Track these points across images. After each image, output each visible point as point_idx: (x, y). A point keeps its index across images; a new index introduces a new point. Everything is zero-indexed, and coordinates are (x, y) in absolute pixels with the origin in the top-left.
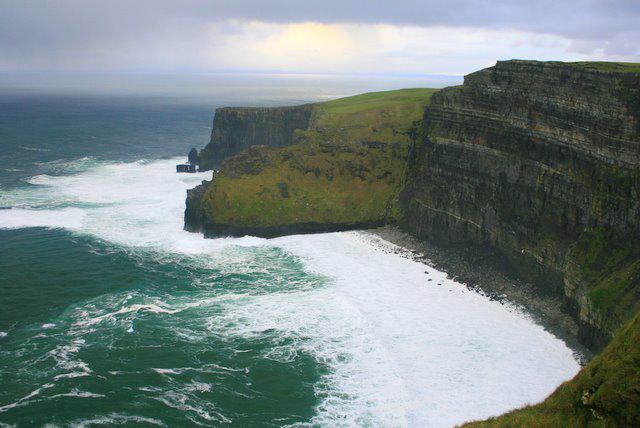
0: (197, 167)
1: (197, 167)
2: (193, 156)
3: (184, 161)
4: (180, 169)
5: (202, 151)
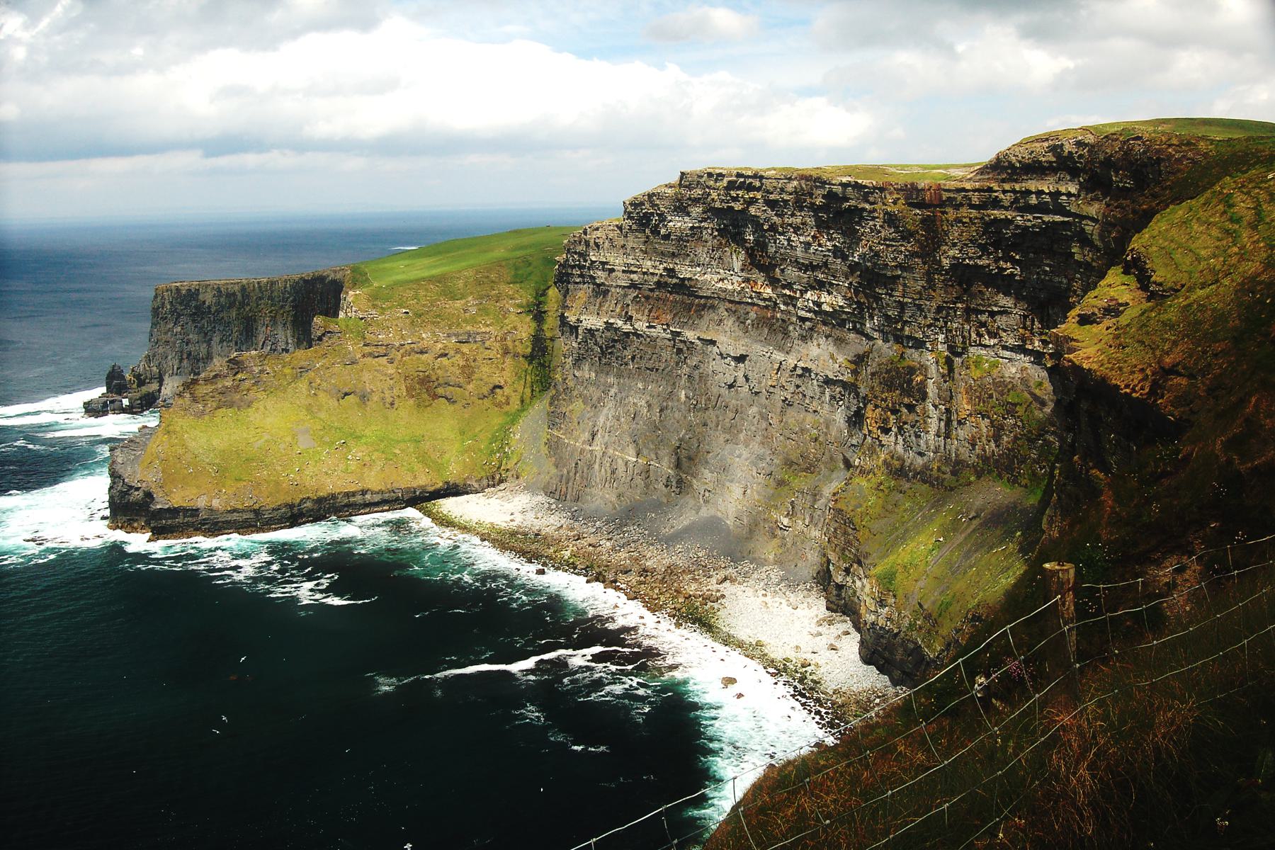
3: (98, 392)
4: (92, 410)
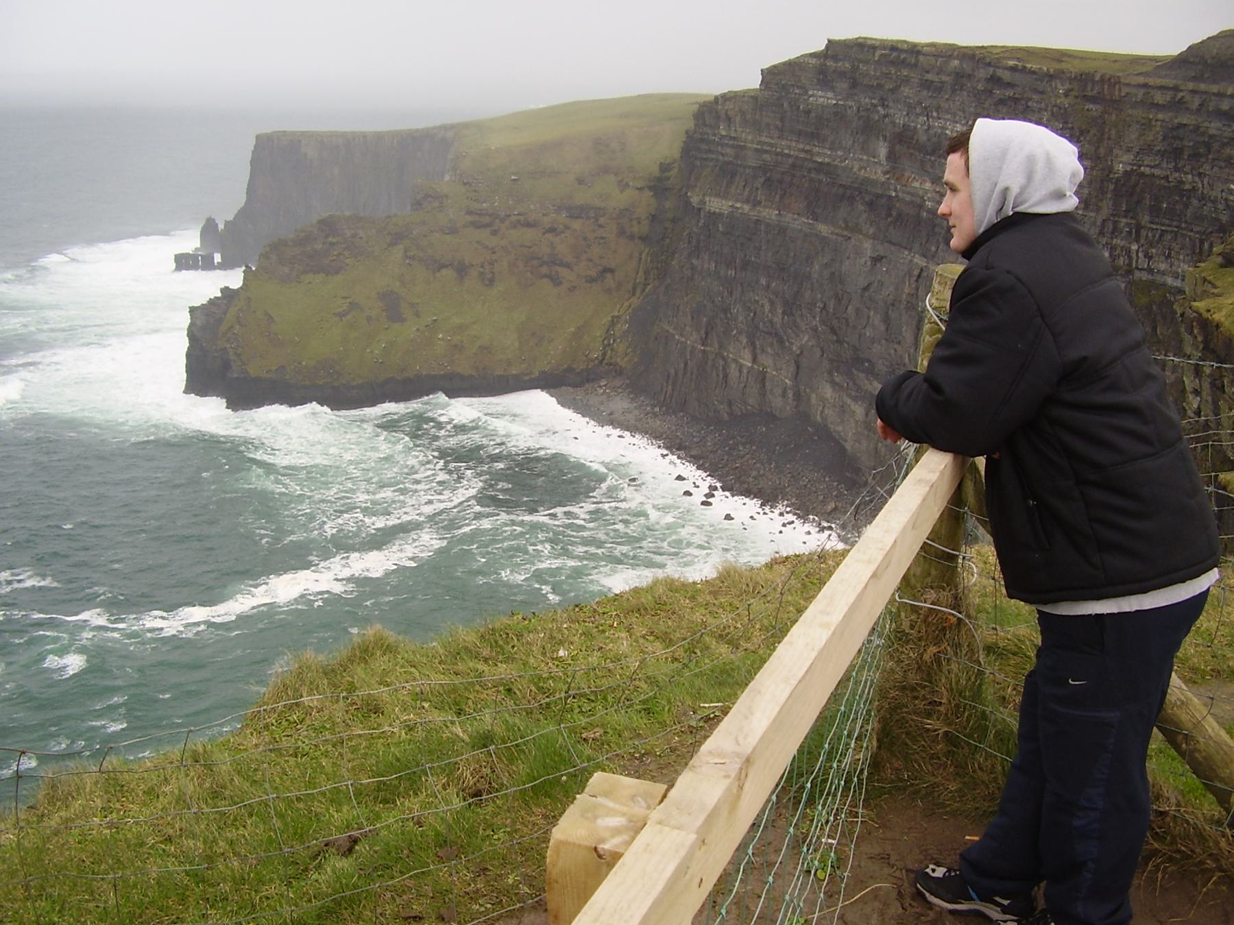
0: (218, 258)
1: (218, 258)
2: (209, 229)
3: (190, 242)
4: (184, 262)
5: (227, 223)
